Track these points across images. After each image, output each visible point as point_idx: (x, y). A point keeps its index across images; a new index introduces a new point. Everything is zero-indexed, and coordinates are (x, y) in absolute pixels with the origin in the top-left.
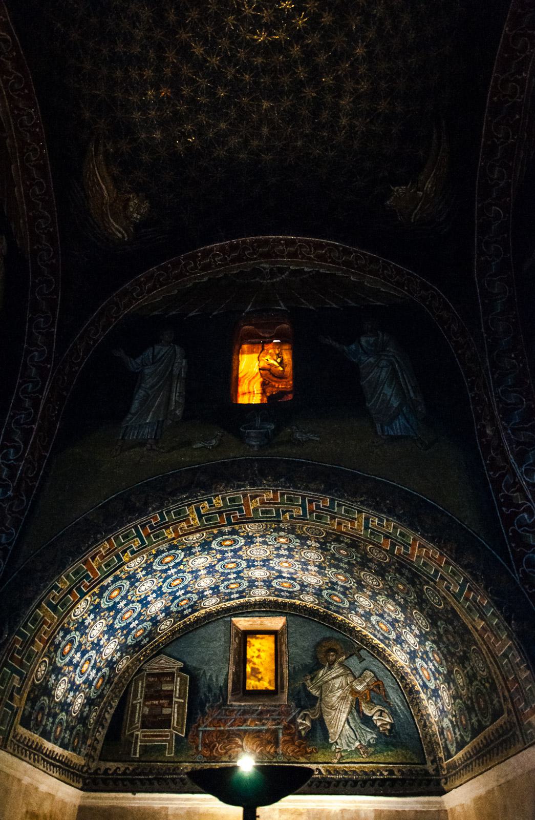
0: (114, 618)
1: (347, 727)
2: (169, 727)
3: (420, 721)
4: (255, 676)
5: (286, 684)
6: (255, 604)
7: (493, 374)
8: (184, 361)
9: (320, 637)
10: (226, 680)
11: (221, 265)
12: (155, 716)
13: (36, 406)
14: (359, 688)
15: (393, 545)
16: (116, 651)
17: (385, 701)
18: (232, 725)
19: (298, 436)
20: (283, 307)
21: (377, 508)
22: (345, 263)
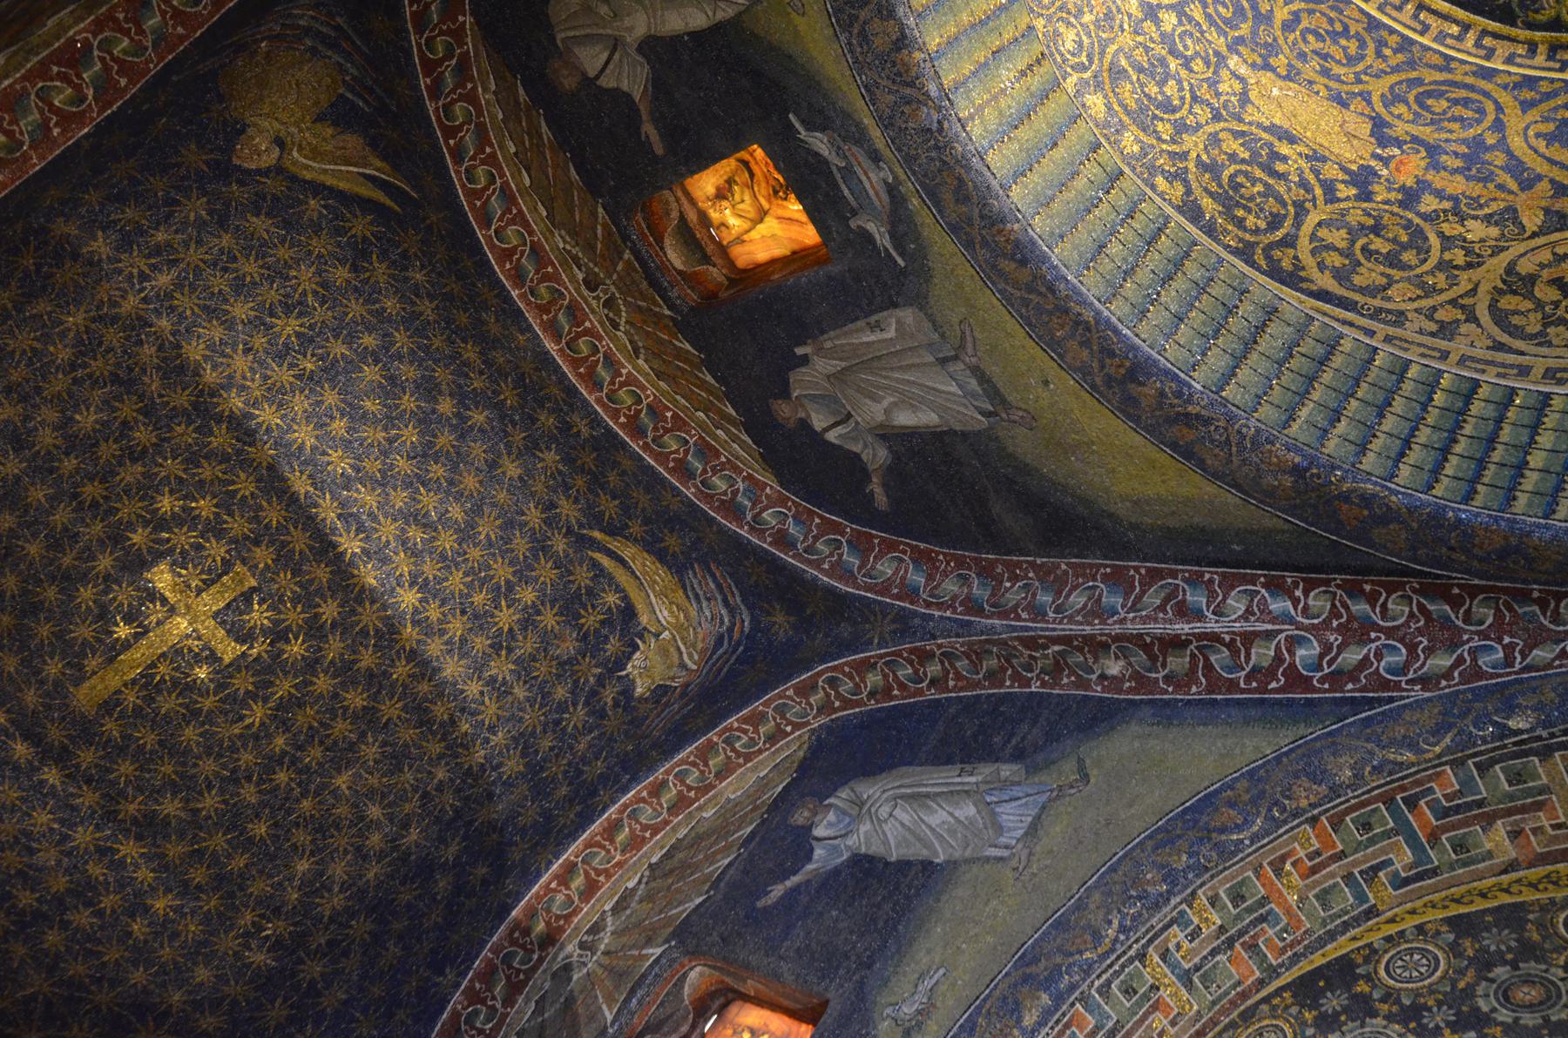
7: (1018, 618)
15: (1252, 947)
19: (908, 1010)
22: (674, 809)
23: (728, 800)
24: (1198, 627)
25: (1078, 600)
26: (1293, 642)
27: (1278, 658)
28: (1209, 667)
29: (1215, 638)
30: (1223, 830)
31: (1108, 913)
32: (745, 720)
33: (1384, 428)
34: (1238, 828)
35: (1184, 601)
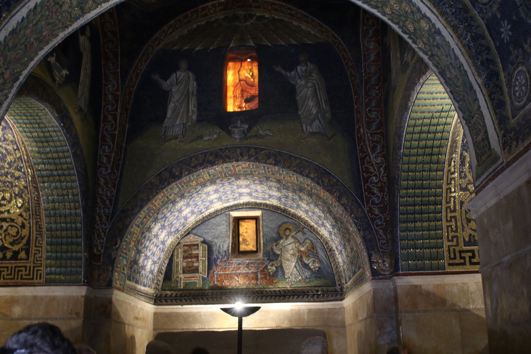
0: (165, 221)
1: (295, 269)
2: (198, 273)
3: (334, 265)
4: (245, 243)
5: (262, 248)
6: (243, 204)
7: (365, 99)
8: (195, 83)
9: (281, 224)
10: (228, 247)
11: (213, 14)
12: (190, 267)
13: (115, 119)
14: (302, 249)
15: (311, 189)
16: (166, 236)
17: (316, 256)
18: (232, 270)
19: (261, 132)
20: (252, 43)
21: (301, 173)
23: (301, 27)
24: (370, 153)
25: (373, 115)
26: (375, 175)
27: (372, 173)
28: (366, 156)
29: (370, 159)
30: (322, 181)
31: (296, 166)
32: (319, 23)
33: (416, 191)
34: (323, 185)
35: (377, 146)
